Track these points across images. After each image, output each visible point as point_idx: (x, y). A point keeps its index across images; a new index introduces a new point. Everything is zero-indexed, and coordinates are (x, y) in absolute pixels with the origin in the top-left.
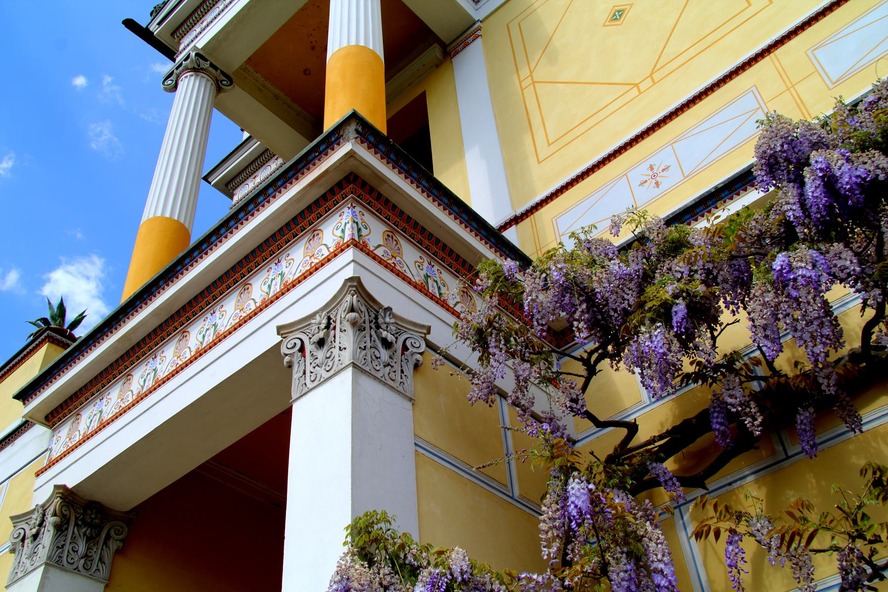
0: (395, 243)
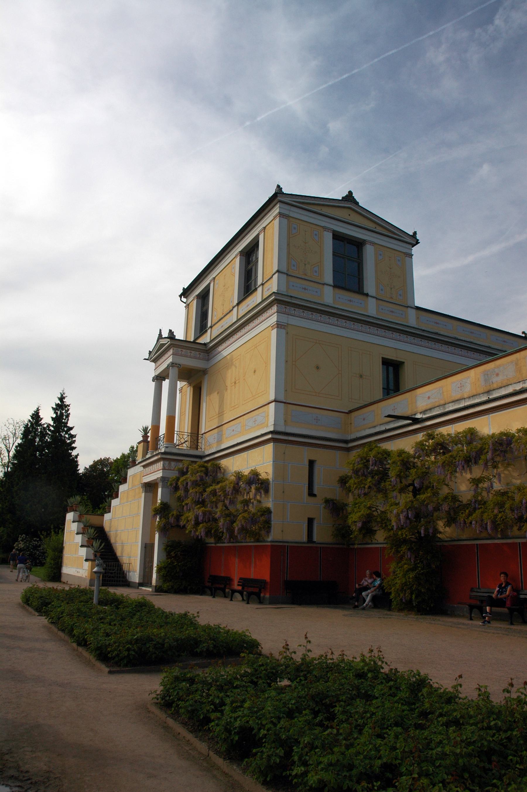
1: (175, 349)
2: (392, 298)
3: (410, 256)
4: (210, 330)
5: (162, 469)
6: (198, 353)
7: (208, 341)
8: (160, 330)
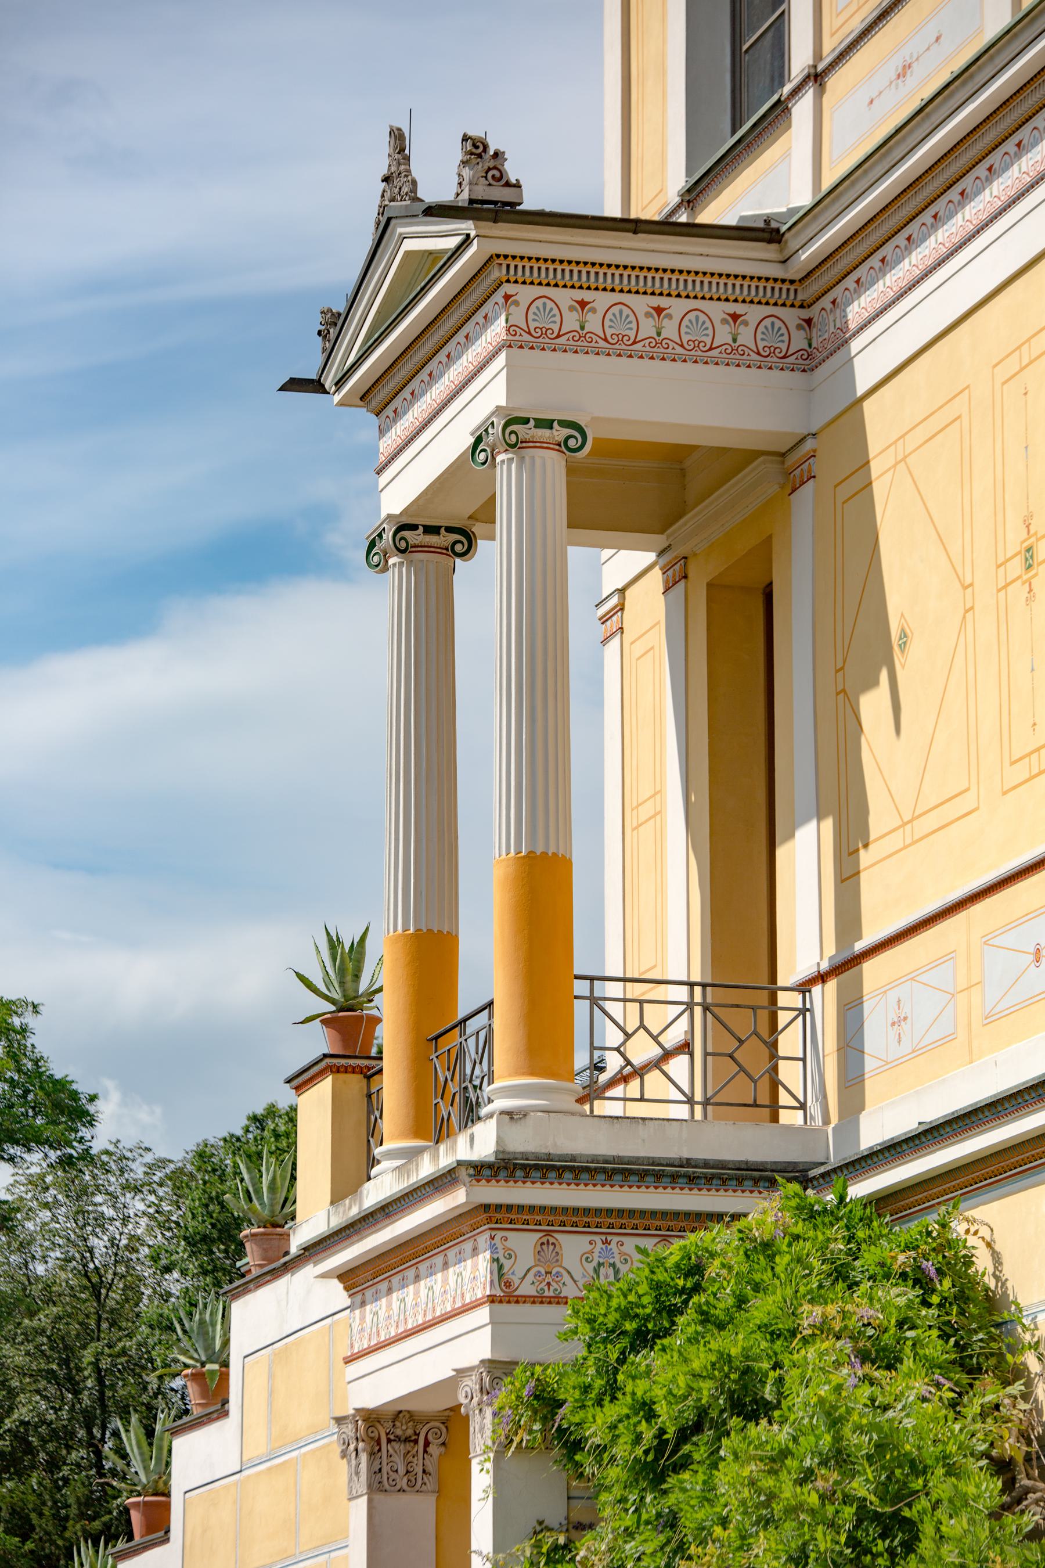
0: (551, 1247)
1: (525, 294)
4: (808, 98)
5: (492, 1300)
6: (717, 310)
7: (803, 197)
8: (399, 139)
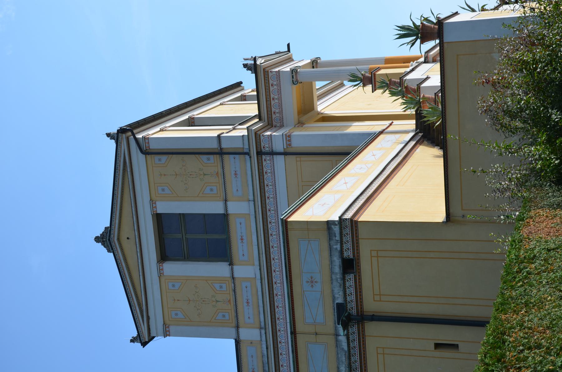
2: (217, 173)
3: (147, 141)
